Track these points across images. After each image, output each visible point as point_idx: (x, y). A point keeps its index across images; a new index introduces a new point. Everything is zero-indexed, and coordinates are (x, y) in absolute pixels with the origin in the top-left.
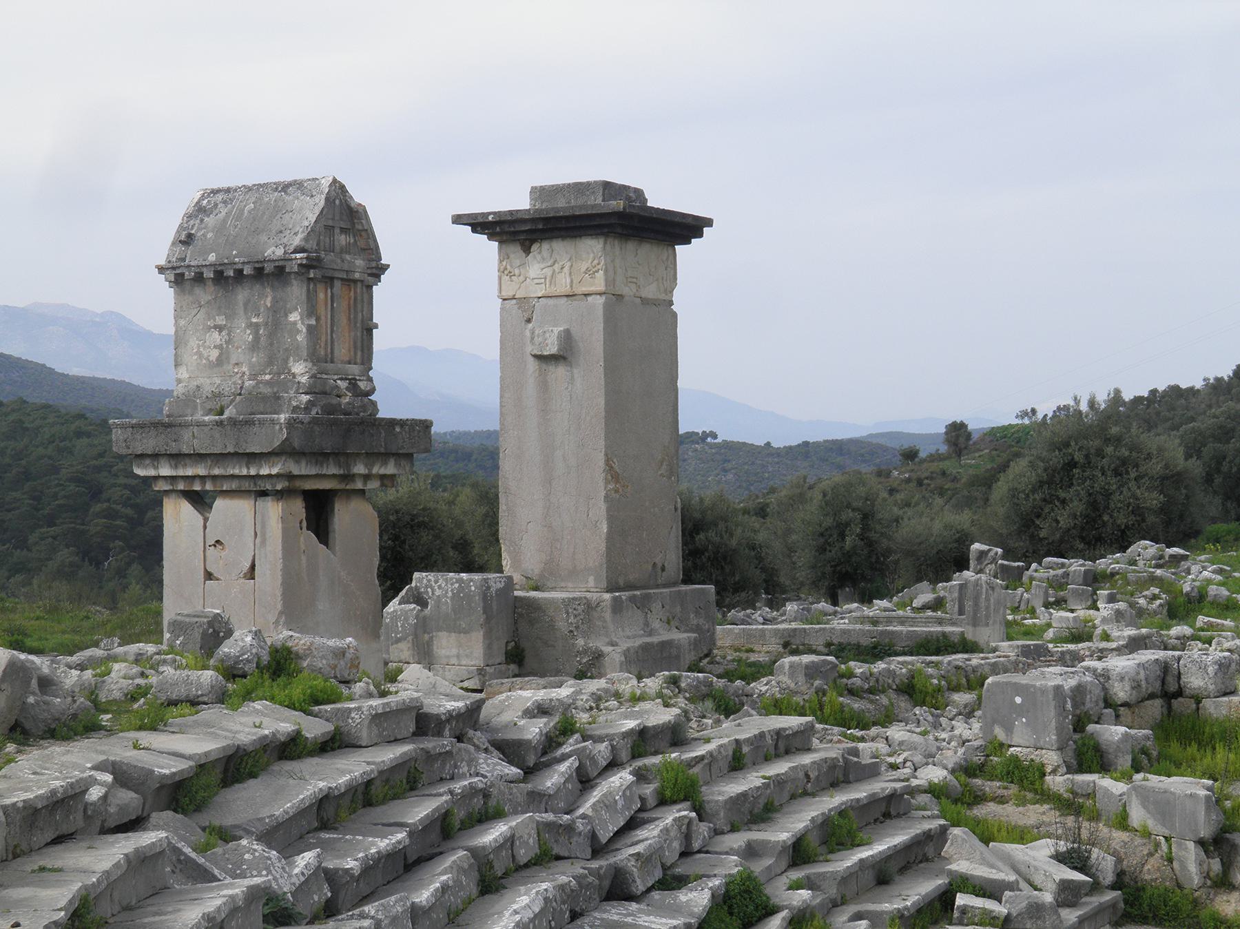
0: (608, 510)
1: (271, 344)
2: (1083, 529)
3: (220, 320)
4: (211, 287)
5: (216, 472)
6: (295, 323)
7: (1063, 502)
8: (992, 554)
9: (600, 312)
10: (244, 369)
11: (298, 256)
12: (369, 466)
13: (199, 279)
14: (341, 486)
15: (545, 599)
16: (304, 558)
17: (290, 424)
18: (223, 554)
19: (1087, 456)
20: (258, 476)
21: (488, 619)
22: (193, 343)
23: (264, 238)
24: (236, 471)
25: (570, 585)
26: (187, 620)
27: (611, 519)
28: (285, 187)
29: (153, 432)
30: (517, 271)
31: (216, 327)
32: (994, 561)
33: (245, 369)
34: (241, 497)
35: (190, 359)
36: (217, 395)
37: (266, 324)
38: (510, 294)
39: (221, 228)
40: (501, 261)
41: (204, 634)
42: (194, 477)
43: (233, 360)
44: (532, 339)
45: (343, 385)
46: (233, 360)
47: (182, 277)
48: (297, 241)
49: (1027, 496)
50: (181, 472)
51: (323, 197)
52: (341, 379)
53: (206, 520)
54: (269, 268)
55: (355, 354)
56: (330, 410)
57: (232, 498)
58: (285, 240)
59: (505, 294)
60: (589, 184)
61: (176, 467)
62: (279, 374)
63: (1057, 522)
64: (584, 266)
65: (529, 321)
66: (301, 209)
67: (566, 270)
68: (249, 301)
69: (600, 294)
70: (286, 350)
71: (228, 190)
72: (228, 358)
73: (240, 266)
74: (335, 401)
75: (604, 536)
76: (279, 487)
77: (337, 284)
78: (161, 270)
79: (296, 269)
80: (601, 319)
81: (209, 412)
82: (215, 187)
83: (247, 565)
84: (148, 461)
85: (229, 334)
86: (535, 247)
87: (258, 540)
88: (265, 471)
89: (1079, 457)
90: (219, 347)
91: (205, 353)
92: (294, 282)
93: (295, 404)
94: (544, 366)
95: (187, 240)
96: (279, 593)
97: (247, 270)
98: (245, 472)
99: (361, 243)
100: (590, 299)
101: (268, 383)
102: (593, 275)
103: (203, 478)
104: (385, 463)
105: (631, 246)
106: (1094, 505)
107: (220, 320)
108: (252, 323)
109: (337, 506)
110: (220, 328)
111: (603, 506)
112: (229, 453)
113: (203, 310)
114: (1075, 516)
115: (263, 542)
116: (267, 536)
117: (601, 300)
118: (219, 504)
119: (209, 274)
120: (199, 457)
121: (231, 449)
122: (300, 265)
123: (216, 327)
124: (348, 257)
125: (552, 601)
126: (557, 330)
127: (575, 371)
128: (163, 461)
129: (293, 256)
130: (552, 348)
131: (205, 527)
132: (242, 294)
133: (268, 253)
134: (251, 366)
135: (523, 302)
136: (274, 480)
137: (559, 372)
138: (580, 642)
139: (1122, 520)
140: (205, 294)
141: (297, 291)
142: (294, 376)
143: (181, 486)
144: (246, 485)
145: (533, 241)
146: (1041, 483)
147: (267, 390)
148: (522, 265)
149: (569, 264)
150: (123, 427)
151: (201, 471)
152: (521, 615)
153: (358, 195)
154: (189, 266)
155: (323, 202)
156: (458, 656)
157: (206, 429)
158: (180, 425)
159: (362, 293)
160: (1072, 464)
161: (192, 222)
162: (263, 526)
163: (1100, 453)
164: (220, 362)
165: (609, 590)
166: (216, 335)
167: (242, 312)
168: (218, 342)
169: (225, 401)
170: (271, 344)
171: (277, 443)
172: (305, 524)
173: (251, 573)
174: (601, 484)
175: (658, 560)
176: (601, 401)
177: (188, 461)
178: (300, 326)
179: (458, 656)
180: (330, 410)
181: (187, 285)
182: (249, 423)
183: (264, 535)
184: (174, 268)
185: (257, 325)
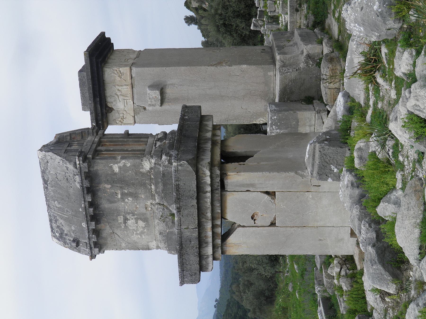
0: (236, 65)
1: (133, 184)
2: (246, 20)
3: (121, 219)
4: (101, 226)
5: (209, 215)
6: (120, 168)
7: (236, 27)
8: (255, 22)
9: (140, 69)
10: (148, 203)
11: (78, 163)
12: (207, 131)
13: (97, 232)
14: (219, 145)
15: (280, 85)
16: (262, 163)
17: (178, 159)
18: (260, 214)
19: (221, 19)
20: (212, 185)
21: (291, 110)
22: (135, 238)
23: (71, 191)
24: (209, 200)
25: (272, 85)
26: (317, 161)
27: (240, 63)
28: (45, 182)
30: (121, 115)
32: (257, 21)
33: (149, 203)
34: (225, 202)
35: (144, 240)
36: (163, 218)
37: (121, 188)
38: (132, 118)
39: (68, 221)
40: (117, 124)
41: (329, 145)
42: (213, 233)
43: (144, 211)
44: (153, 105)
45: (158, 143)
46: (143, 210)
47: (96, 243)
48: (71, 167)
49: (235, 39)
50: (210, 240)
51: (47, 154)
52: (155, 145)
53: (240, 226)
54: (87, 184)
55: (142, 142)
56: (171, 147)
57: (225, 208)
58: (71, 175)
59: (132, 122)
60: (80, 80)
61: (207, 243)
62: (151, 179)
63: (243, 28)
64: (118, 79)
65: (145, 109)
66: (55, 168)
67: (120, 88)
68: (108, 200)
69: (131, 70)
70: (136, 174)
71: (51, 221)
72: (143, 214)
73: (87, 203)
74: (168, 145)
75: (248, 67)
76: (218, 172)
77: (99, 148)
78: (93, 257)
79: (86, 164)
80: (143, 69)
81: (173, 222)
82: (50, 230)
83: (266, 197)
84: (204, 262)
85: (129, 213)
86: (109, 105)
87: (251, 189)
88: (208, 180)
89: (221, 22)
90: (137, 219)
91: (141, 230)
92: (95, 168)
93: (167, 163)
94: (166, 100)
95: (76, 244)
96: (284, 175)
97: (89, 199)
98: (209, 195)
99: (79, 138)
100: (133, 76)
101: (156, 187)
102: (122, 74)
104: (206, 125)
105: (110, 61)
106: (238, 16)
107: (121, 219)
108: (121, 198)
109: (231, 150)
111: (234, 67)
112: (198, 203)
113: (116, 231)
114: (241, 22)
115: (253, 185)
116: (248, 182)
117: (134, 69)
119: (93, 225)
120: (200, 226)
121: (195, 202)
122: (84, 162)
123: (125, 223)
124: (85, 144)
125: (281, 81)
126: (149, 91)
127: (168, 83)
128: (204, 252)
129: (78, 166)
130: (156, 94)
131: (244, 226)
132: (105, 205)
133: (78, 186)
134: (147, 198)
135: (136, 112)
136: (214, 176)
137: (169, 91)
138: (302, 65)
139: (243, 6)
140: (106, 229)
141: (100, 166)
142: (151, 168)
143: (219, 241)
144: (217, 196)
145: (107, 106)
146: (231, 35)
148: (118, 112)
149: (117, 87)
151: (209, 225)
152: (288, 99)
153: (50, 138)
154: (89, 238)
155: (50, 154)
156: (310, 126)
157: (183, 219)
158: (181, 238)
159: (108, 138)
160: (224, 24)
161: (68, 241)
162: (243, 185)
163: (221, 15)
164: (145, 220)
165: (274, 62)
167: (115, 205)
168: (134, 221)
169: (167, 213)
170: (133, 184)
171: (190, 168)
172: (242, 163)
173: (271, 194)
174: (223, 68)
175: (259, 51)
176: (183, 68)
177: (203, 235)
178: (121, 164)
179: (310, 126)
180: (171, 147)
181: (101, 241)
182: (178, 188)
183: (248, 185)
184: (91, 248)
185: (123, 194)
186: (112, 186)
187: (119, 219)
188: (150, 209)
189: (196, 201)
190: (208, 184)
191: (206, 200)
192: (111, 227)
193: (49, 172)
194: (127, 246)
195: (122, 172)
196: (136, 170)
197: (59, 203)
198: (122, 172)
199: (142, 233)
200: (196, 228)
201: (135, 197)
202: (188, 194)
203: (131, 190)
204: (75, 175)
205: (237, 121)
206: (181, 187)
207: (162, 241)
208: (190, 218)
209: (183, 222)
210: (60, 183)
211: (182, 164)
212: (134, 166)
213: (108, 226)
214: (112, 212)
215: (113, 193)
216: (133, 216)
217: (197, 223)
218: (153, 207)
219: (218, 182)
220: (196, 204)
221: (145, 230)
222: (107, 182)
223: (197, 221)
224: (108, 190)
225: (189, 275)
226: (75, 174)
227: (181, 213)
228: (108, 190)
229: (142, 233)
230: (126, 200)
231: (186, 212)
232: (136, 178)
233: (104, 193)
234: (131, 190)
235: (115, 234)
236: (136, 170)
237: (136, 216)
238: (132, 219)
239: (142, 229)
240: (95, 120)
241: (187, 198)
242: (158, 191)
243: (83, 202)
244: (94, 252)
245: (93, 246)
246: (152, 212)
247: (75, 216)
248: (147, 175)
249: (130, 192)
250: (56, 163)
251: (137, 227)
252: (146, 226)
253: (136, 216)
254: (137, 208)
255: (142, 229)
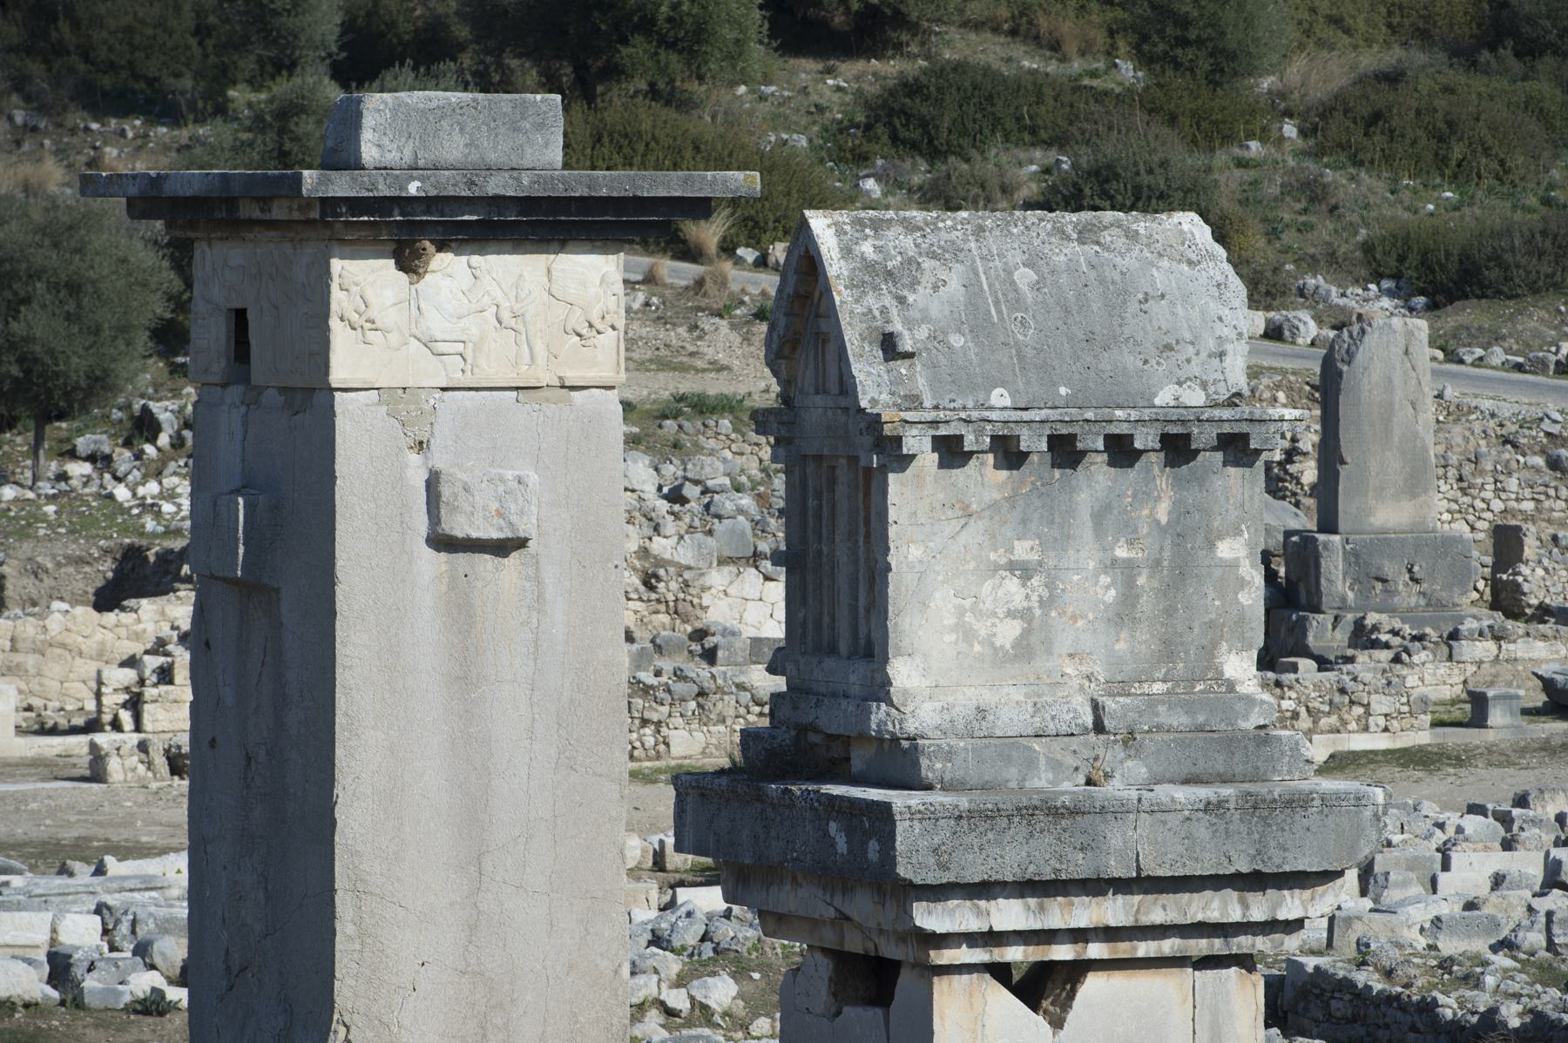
6: (1234, 565)
29: (1019, 829)
31: (1012, 567)
37: (1158, 563)
46: (1064, 643)
62: (1193, 681)
70: (1211, 625)
72: (1048, 646)
73: (1123, 429)
90: (1025, 615)
91: (982, 629)
103: (1079, 936)
107: (1024, 550)
108: (1114, 561)
110: (1024, 571)
118: (1093, 986)
123: (1012, 567)
147: (1179, 720)
150: (929, 816)
164: (1023, 650)
166: (1012, 584)
168: (1018, 601)
170: (1170, 612)
185: (1130, 567)
186: (1162, 530)
187: (1027, 544)
188: (1069, 671)
189: (1245, 869)
190: (1274, 909)
191: (1215, 904)
192: (994, 506)
193: (1152, 264)
194: (911, 567)
195: (1217, 572)
196: (1223, 625)
197: (1037, 287)
198: (1217, 572)
199: (968, 635)
200: (1139, 869)
201: (1119, 615)
202: (1273, 844)
203: (1146, 603)
204: (1204, 386)
205: (350, 938)
206: (1297, 817)
207: (947, 717)
208: (1180, 848)
209: (1164, 823)
210: (1133, 307)
211: (1379, 820)
212: (1241, 620)
213: (997, 496)
214: (1057, 520)
215: (1135, 531)
216: (1041, 601)
217: (1160, 873)
218: (1075, 683)
219: (1253, 946)
220: (1232, 870)
221: (977, 648)
222: (1181, 511)
223: (1170, 874)
224: (1146, 512)
225: (937, 840)
226: (1212, 389)
227: (1201, 814)
228: (1146, 512)
229: (968, 635)
230: (1105, 580)
231: (1202, 832)
232: (1196, 625)
233: (1134, 496)
234: (1146, 603)
235: (963, 521)
236: (1223, 625)
237: (1038, 612)
238: (1027, 597)
239: (983, 633)
240: (433, 193)
241: (1257, 836)
242: (1160, 708)
243: (1134, 415)
244: (915, 432)
245: (943, 431)
246: (1059, 679)
247: (1021, 357)
248: (1208, 668)
249: (1138, 596)
250: (1214, 308)
251: (994, 614)
252: (995, 649)
253: (1038, 612)
254: (1074, 618)
255: (983, 633)
